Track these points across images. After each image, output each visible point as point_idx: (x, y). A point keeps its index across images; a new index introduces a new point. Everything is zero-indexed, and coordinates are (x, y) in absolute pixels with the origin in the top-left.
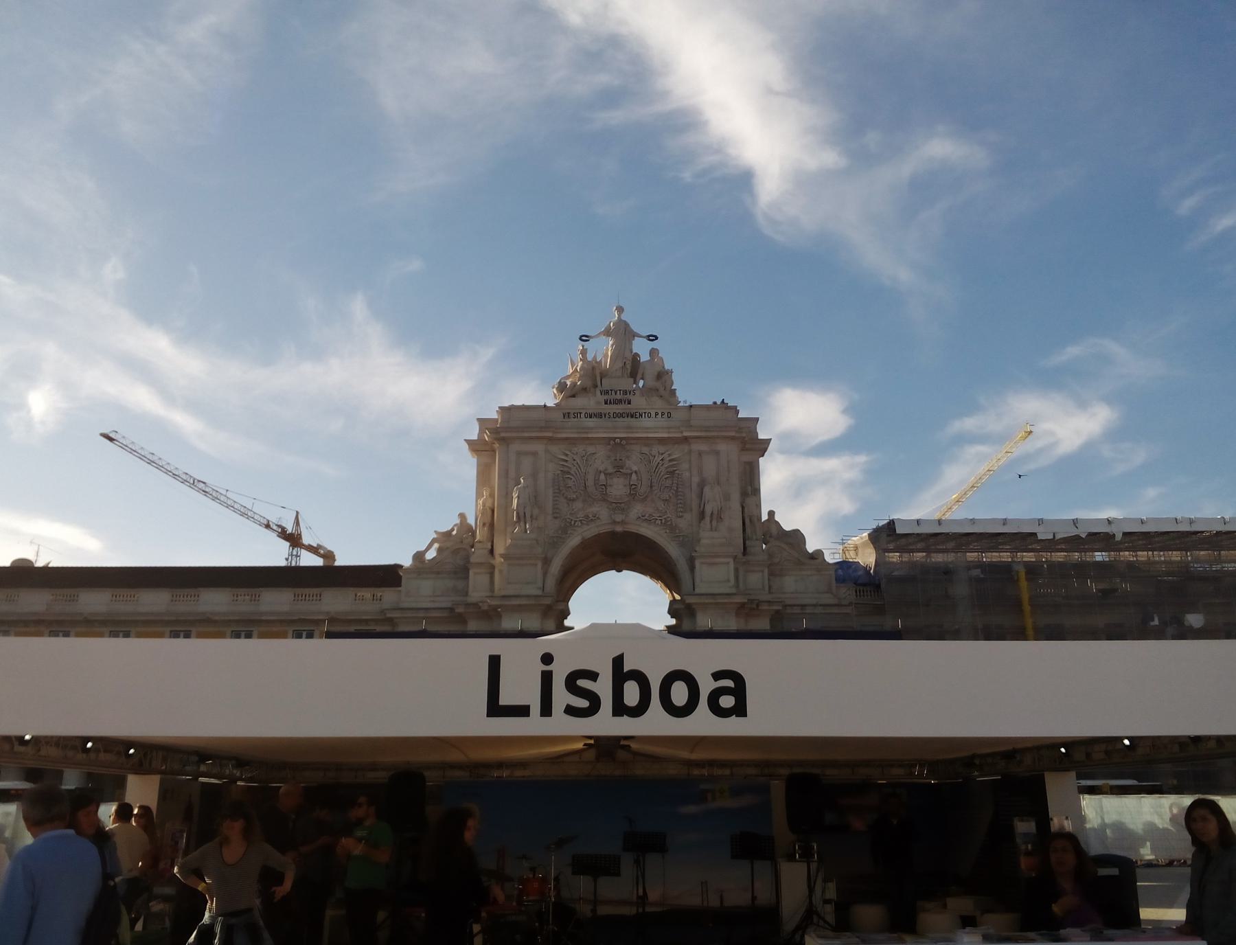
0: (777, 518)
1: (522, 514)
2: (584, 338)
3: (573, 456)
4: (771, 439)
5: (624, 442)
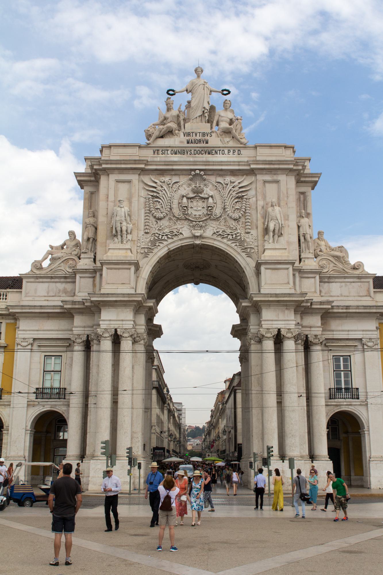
0: (325, 237)
1: (119, 229)
2: (171, 93)
3: (161, 184)
4: (321, 174)
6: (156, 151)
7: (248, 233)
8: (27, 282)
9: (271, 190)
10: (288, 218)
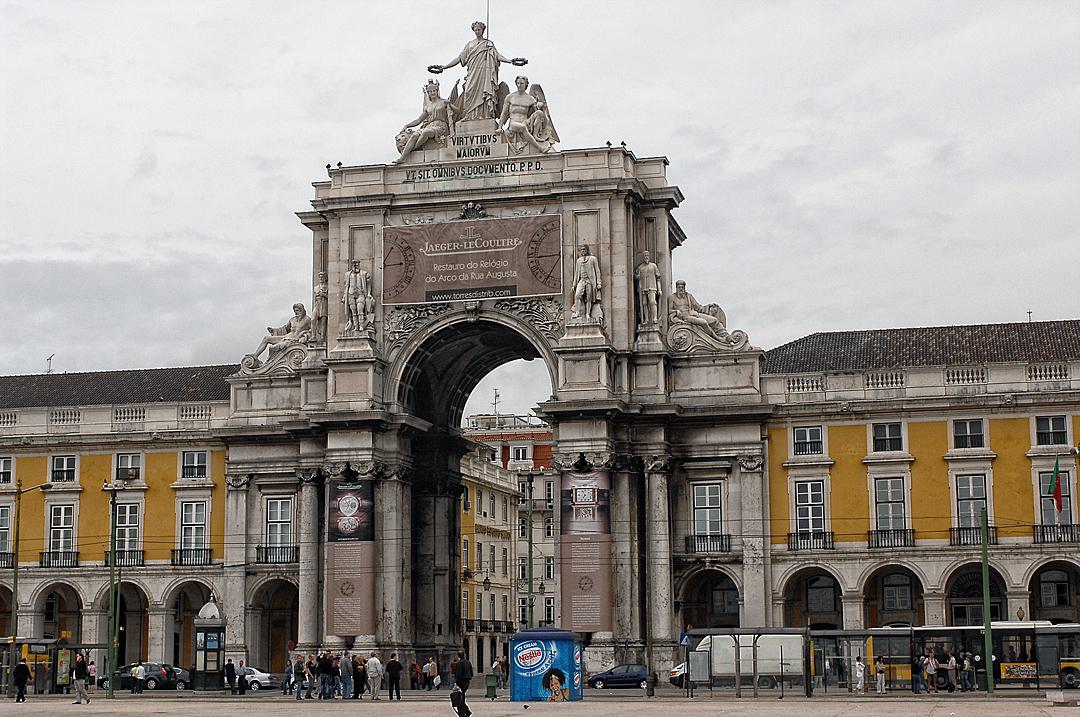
2: (436, 70)
6: (412, 174)
9: (586, 230)
10: (611, 270)
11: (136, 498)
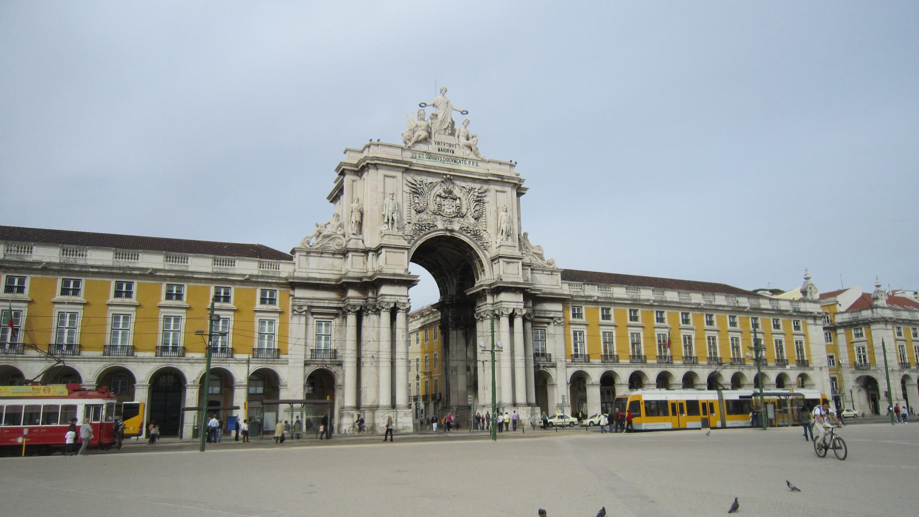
1: (390, 218)
5: (452, 177)
7: (485, 231)
8: (300, 255)
11: (227, 315)
